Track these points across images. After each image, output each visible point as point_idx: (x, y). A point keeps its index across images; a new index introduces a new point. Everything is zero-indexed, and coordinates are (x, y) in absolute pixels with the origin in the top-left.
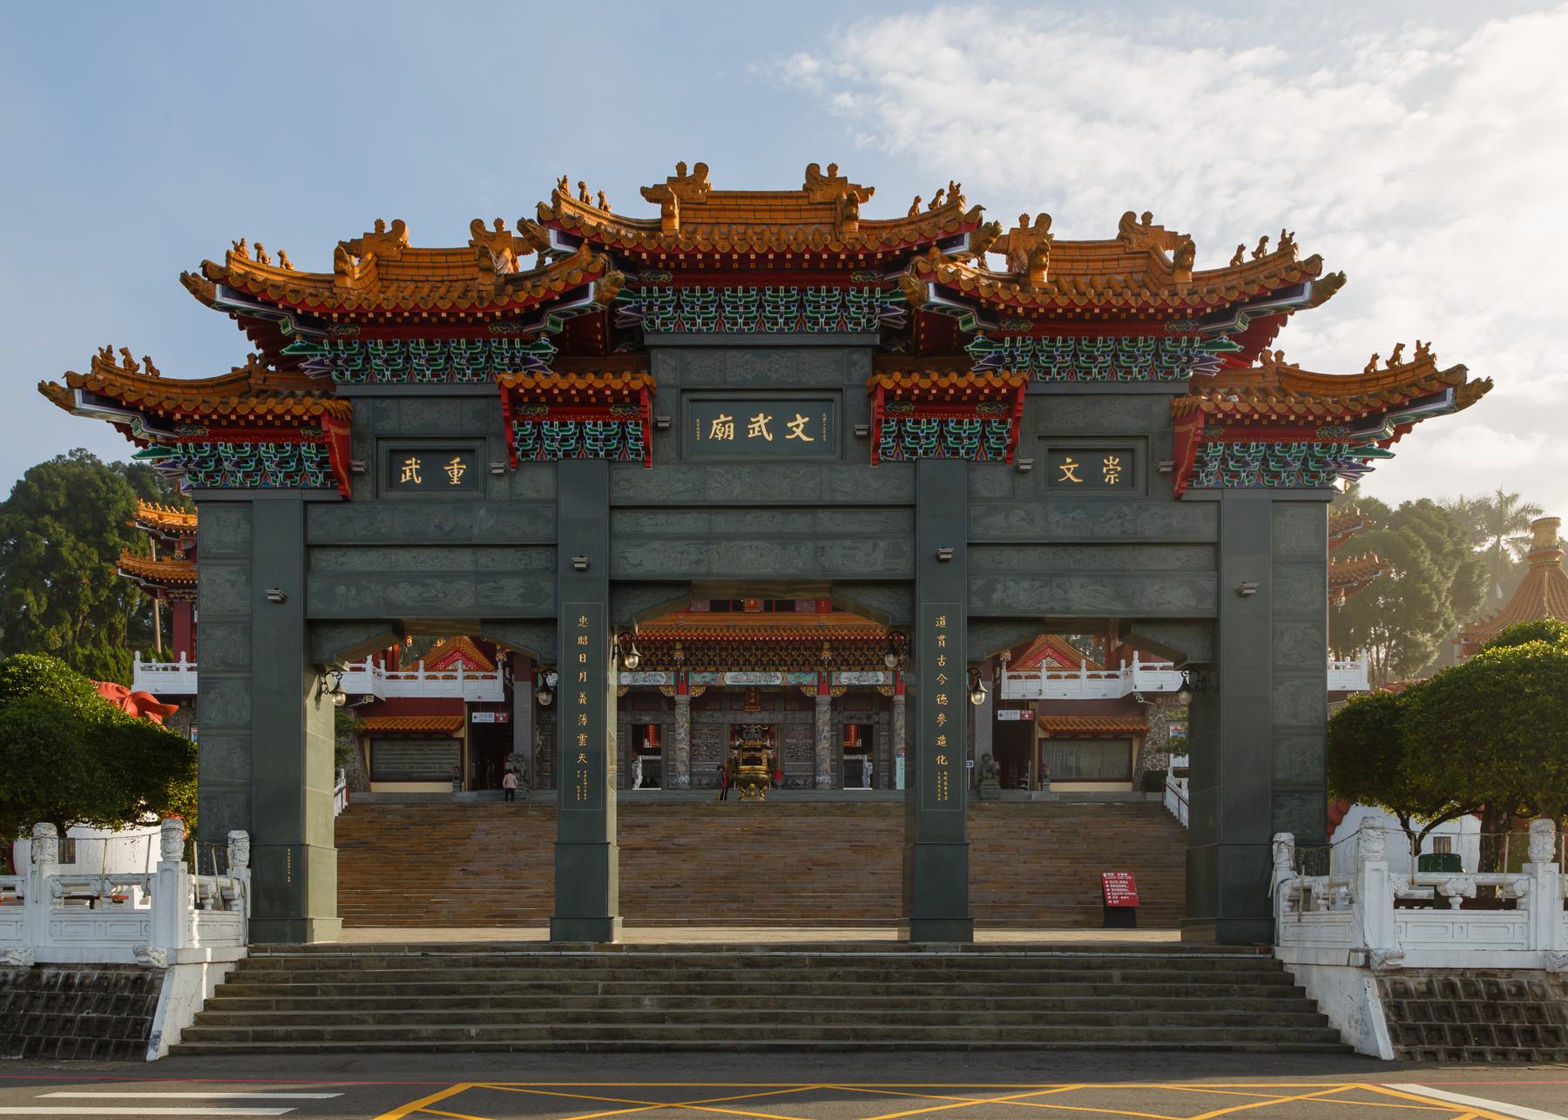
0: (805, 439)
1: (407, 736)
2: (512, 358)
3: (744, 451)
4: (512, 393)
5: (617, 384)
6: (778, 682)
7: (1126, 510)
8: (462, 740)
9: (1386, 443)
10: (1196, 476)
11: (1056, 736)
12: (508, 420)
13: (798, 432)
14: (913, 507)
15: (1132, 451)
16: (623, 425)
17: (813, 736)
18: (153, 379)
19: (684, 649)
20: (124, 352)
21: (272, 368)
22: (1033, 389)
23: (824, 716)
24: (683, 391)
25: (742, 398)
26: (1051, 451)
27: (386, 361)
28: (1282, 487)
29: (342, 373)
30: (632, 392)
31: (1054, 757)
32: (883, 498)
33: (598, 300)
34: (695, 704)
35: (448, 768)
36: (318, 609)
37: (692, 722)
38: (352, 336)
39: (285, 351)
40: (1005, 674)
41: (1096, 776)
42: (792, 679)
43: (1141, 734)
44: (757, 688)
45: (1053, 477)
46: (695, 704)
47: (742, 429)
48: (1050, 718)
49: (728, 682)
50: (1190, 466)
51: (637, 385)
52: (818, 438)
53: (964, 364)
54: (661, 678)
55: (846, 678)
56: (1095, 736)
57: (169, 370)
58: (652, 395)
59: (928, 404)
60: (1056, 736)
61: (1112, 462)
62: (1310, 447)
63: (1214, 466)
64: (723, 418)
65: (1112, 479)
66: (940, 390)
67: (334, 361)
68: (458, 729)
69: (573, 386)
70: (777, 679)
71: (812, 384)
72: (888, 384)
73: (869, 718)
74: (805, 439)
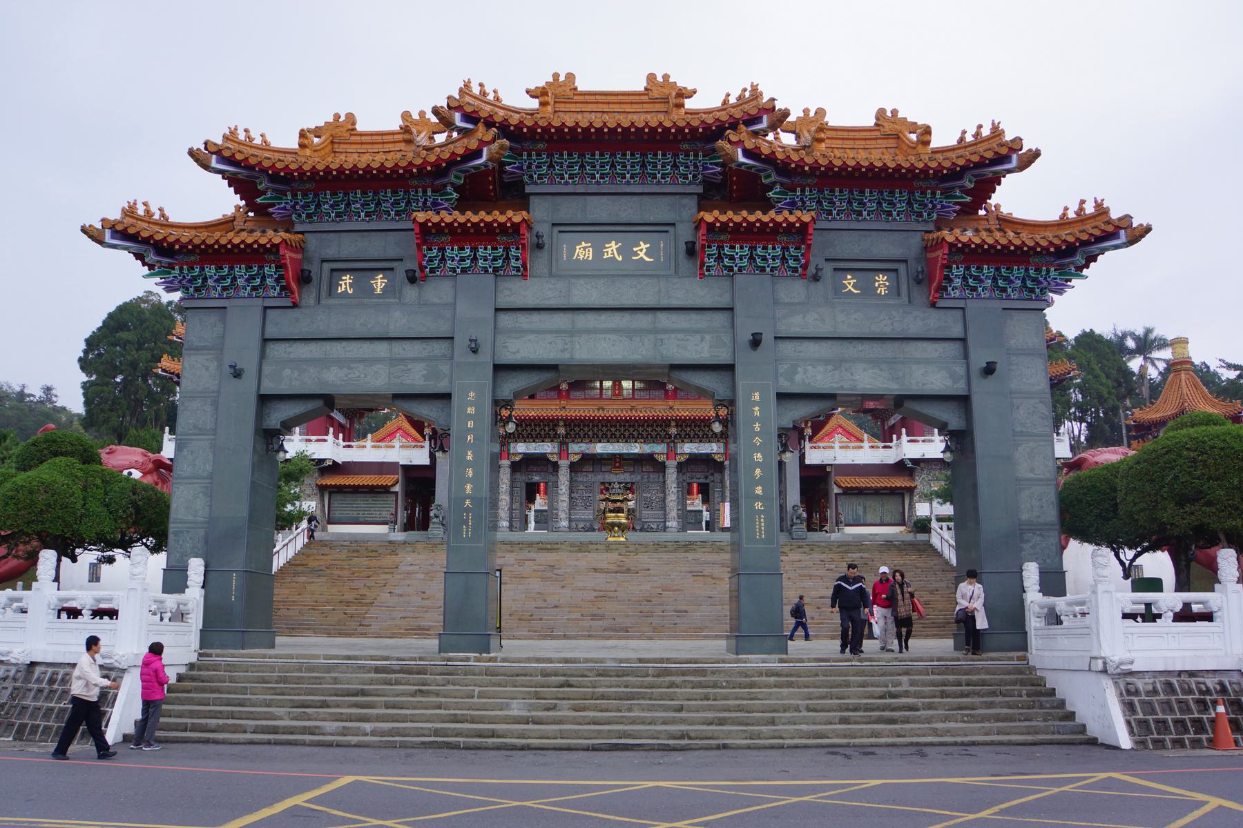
0: (647, 259)
1: (356, 490)
2: (425, 203)
3: (599, 271)
4: (423, 226)
5: (502, 219)
6: (636, 451)
7: (894, 313)
8: (396, 493)
9: (1080, 269)
10: (945, 289)
12: (419, 246)
13: (642, 254)
14: (732, 309)
15: (896, 270)
16: (507, 249)
17: (664, 492)
18: (165, 223)
19: (565, 426)
20: (145, 204)
21: (251, 214)
22: (820, 225)
23: (671, 476)
24: (554, 225)
25: (600, 228)
26: (835, 269)
27: (332, 206)
28: (1008, 298)
29: (300, 216)
30: (513, 224)
31: (848, 508)
32: (708, 302)
33: (489, 160)
34: (574, 467)
35: (386, 515)
36: (269, 387)
37: (571, 481)
38: (308, 190)
39: (259, 200)
40: (808, 445)
42: (647, 448)
43: (911, 490)
44: (621, 455)
45: (838, 289)
46: (574, 467)
47: (598, 252)
49: (599, 451)
50: (940, 283)
51: (517, 219)
52: (657, 259)
53: (767, 206)
54: (547, 448)
55: (689, 448)
57: (177, 215)
58: (530, 228)
59: (740, 234)
60: (848, 492)
61: (881, 278)
62: (1027, 270)
63: (958, 282)
64: (584, 244)
65: (882, 291)
66: (748, 223)
67: (293, 207)
68: (393, 485)
69: (468, 220)
70: (636, 448)
71: (652, 220)
72: (709, 218)
73: (706, 478)
74: (647, 259)
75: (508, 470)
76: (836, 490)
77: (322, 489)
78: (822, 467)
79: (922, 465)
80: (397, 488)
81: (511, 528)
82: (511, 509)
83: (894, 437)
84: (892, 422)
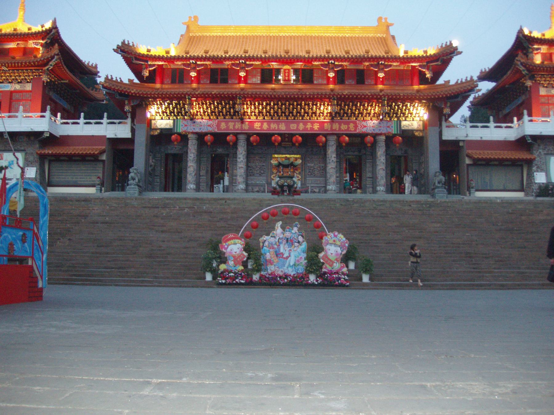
1: (71, 159)
8: (103, 161)
11: (478, 163)
31: (476, 176)
40: (444, 124)
41: (502, 188)
43: (529, 162)
48: (474, 151)
56: (502, 163)
60: (478, 163)
73: (360, 151)
75: (195, 142)
76: (468, 161)
77: (42, 158)
78: (455, 143)
79: (539, 141)
80: (104, 157)
81: (198, 189)
82: (198, 175)
83: (515, 119)
84: (507, 111)
